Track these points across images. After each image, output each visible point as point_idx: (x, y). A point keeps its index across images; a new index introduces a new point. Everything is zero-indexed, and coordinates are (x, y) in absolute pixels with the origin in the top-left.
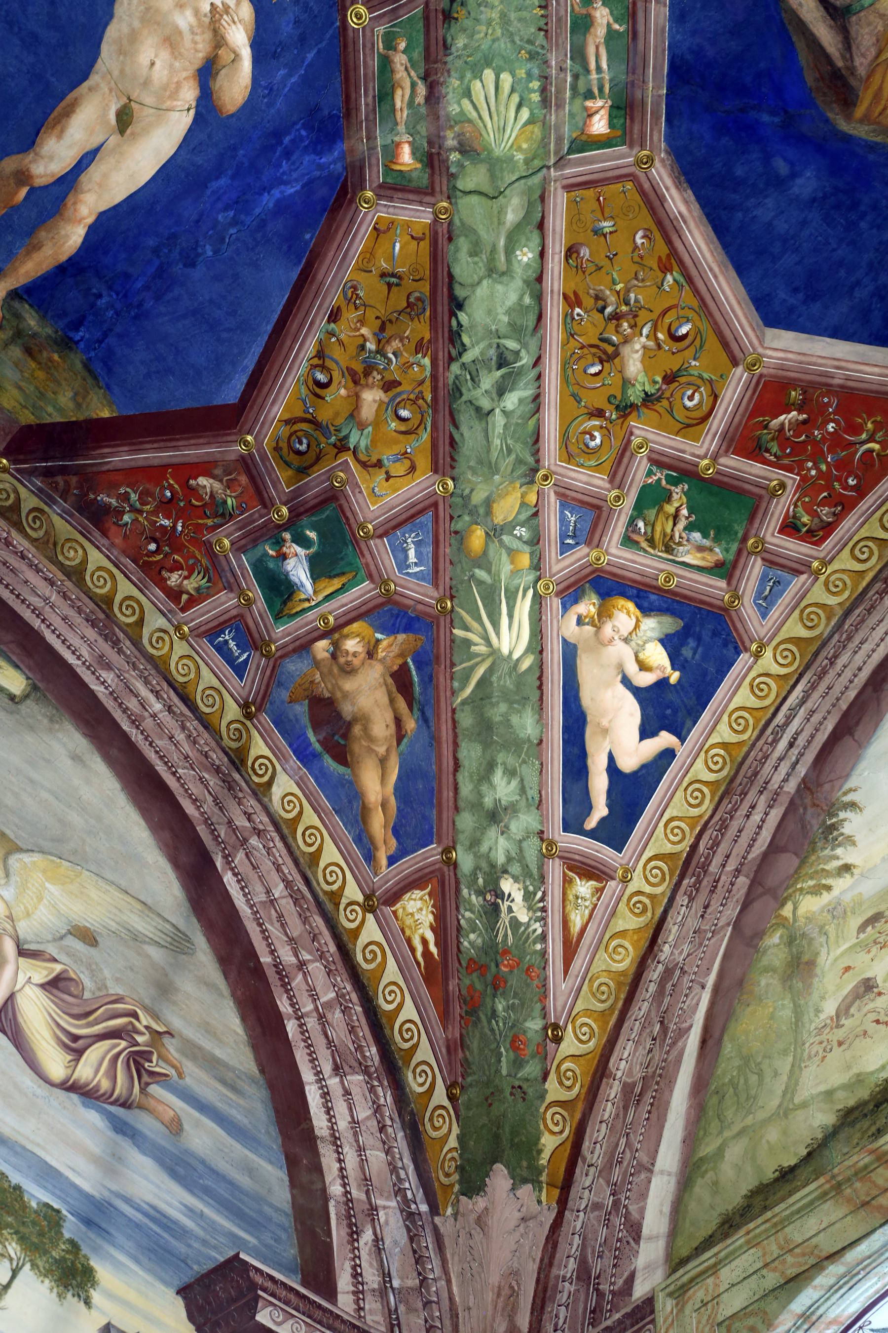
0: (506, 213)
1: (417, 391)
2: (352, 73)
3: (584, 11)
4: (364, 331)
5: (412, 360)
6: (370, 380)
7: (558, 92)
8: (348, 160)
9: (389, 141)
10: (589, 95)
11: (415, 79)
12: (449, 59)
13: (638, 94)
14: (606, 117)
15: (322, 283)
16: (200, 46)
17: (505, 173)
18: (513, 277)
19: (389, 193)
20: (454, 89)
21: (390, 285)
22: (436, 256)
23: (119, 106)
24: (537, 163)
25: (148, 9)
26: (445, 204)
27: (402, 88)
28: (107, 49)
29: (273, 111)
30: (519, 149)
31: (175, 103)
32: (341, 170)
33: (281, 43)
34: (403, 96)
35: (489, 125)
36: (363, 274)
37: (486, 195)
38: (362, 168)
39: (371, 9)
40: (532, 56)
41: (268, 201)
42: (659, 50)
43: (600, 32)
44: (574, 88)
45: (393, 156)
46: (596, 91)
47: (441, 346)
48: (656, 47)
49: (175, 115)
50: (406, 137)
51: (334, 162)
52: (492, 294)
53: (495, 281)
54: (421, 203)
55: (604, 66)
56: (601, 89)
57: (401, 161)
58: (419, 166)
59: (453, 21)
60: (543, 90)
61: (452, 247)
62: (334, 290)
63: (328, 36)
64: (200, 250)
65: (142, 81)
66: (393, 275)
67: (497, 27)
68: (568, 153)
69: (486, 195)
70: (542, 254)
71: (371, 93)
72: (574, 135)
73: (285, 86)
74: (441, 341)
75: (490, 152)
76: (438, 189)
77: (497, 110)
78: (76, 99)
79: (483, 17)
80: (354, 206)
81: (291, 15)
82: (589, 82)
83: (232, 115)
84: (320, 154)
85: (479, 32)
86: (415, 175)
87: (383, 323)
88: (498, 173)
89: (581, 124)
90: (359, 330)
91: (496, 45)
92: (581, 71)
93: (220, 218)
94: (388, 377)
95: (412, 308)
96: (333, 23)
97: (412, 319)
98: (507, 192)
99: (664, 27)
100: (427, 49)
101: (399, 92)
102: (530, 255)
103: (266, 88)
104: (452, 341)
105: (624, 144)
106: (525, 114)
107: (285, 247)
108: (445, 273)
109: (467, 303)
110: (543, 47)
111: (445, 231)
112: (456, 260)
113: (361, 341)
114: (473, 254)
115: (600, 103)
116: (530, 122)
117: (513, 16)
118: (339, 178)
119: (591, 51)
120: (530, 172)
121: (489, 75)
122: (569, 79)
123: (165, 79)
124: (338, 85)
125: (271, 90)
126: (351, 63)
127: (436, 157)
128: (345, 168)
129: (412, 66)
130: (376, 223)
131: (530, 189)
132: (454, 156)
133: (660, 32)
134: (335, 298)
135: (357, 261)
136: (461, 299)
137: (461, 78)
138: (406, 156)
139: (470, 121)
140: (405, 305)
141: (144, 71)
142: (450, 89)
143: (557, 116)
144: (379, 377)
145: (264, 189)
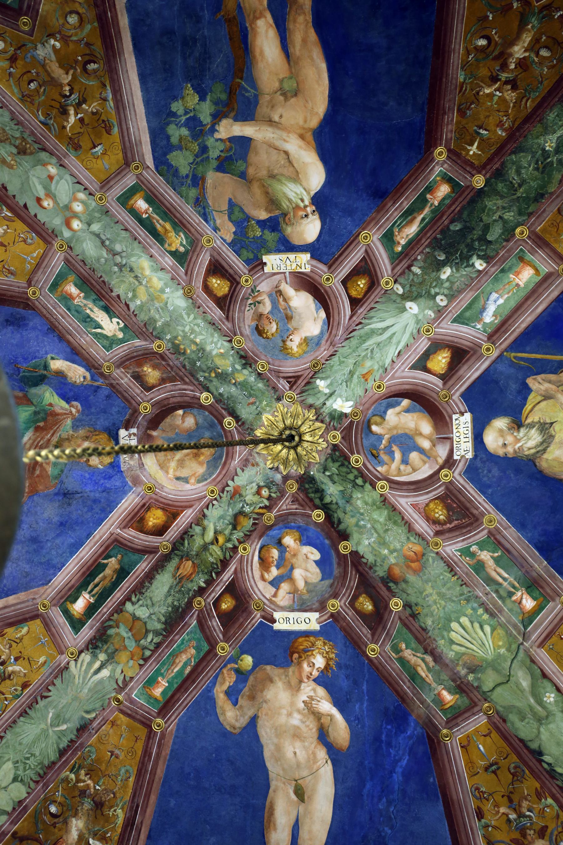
0: (521, 684)
1: (559, 824)
2: (390, 679)
3: (475, 561)
4: (502, 810)
5: (541, 807)
6: (529, 838)
7: (494, 605)
8: (421, 722)
9: (433, 696)
10: (511, 594)
11: (422, 656)
12: (430, 634)
13: (534, 574)
14: (528, 597)
15: (459, 800)
16: (311, 726)
17: (503, 664)
18: (554, 715)
19: (454, 722)
20: (444, 646)
21: (494, 772)
22: (505, 736)
23: (293, 788)
24: (514, 646)
25: (276, 729)
26: (487, 705)
27: (419, 666)
28: (269, 765)
29: (366, 729)
30: (499, 647)
31: (318, 764)
32: (421, 731)
33: (346, 692)
34: (422, 669)
35: (475, 648)
36: (475, 777)
37: (503, 683)
38: (430, 721)
39: (376, 643)
40: (468, 600)
41: (397, 777)
42: (525, 547)
43: (491, 563)
44: (500, 597)
45: (441, 702)
46: (513, 590)
47: (550, 785)
48: (522, 547)
49: (322, 771)
50: (440, 688)
51: (415, 729)
52: (551, 732)
53: (547, 724)
54: (474, 714)
55: (506, 575)
56: (514, 587)
57: (446, 702)
58: (457, 696)
59: (418, 616)
60: (487, 610)
61: (509, 724)
62: (468, 799)
63: (366, 671)
64: (383, 834)
65: (295, 766)
66: (492, 765)
67: (440, 601)
68: (525, 629)
69: (503, 683)
70: (558, 690)
71: (406, 681)
72: (521, 618)
73: (363, 711)
74: (547, 782)
75: (486, 660)
76: (476, 700)
77: (472, 638)
78: (271, 802)
79: (430, 602)
80: (442, 744)
81: (342, 676)
82: (505, 589)
83: (349, 747)
84: (404, 731)
85: (434, 611)
86: (459, 702)
87: (509, 797)
88: (500, 668)
89: (519, 610)
90: (498, 812)
91: (446, 609)
92: (497, 587)
93: (381, 807)
94: (537, 828)
95: (516, 776)
96: (364, 663)
97: (522, 782)
98: (512, 673)
99: (519, 537)
100: (416, 638)
101: (419, 669)
102: (553, 695)
103: (355, 720)
104: (553, 778)
105: (549, 602)
106: (487, 629)
107: (425, 796)
108: (517, 741)
109: (542, 749)
110: (470, 592)
111: (498, 719)
112: (517, 729)
113: (505, 818)
114: (523, 719)
115: (519, 594)
116: (493, 630)
117: (444, 590)
118: (423, 735)
119: (494, 574)
120: (515, 653)
121: (454, 625)
122: (494, 595)
123: (306, 756)
124: (388, 690)
125: (358, 719)
126: (386, 674)
127: (462, 685)
128: (423, 728)
129: (416, 651)
130: (460, 744)
131: (523, 662)
132: (471, 677)
133: (519, 540)
134: (472, 804)
135: (467, 773)
136: (537, 749)
137: (443, 638)
138: (447, 697)
139: (464, 654)
140: (511, 776)
141: (294, 760)
142: (442, 647)
143: (504, 617)
144: (532, 832)
145: (392, 772)
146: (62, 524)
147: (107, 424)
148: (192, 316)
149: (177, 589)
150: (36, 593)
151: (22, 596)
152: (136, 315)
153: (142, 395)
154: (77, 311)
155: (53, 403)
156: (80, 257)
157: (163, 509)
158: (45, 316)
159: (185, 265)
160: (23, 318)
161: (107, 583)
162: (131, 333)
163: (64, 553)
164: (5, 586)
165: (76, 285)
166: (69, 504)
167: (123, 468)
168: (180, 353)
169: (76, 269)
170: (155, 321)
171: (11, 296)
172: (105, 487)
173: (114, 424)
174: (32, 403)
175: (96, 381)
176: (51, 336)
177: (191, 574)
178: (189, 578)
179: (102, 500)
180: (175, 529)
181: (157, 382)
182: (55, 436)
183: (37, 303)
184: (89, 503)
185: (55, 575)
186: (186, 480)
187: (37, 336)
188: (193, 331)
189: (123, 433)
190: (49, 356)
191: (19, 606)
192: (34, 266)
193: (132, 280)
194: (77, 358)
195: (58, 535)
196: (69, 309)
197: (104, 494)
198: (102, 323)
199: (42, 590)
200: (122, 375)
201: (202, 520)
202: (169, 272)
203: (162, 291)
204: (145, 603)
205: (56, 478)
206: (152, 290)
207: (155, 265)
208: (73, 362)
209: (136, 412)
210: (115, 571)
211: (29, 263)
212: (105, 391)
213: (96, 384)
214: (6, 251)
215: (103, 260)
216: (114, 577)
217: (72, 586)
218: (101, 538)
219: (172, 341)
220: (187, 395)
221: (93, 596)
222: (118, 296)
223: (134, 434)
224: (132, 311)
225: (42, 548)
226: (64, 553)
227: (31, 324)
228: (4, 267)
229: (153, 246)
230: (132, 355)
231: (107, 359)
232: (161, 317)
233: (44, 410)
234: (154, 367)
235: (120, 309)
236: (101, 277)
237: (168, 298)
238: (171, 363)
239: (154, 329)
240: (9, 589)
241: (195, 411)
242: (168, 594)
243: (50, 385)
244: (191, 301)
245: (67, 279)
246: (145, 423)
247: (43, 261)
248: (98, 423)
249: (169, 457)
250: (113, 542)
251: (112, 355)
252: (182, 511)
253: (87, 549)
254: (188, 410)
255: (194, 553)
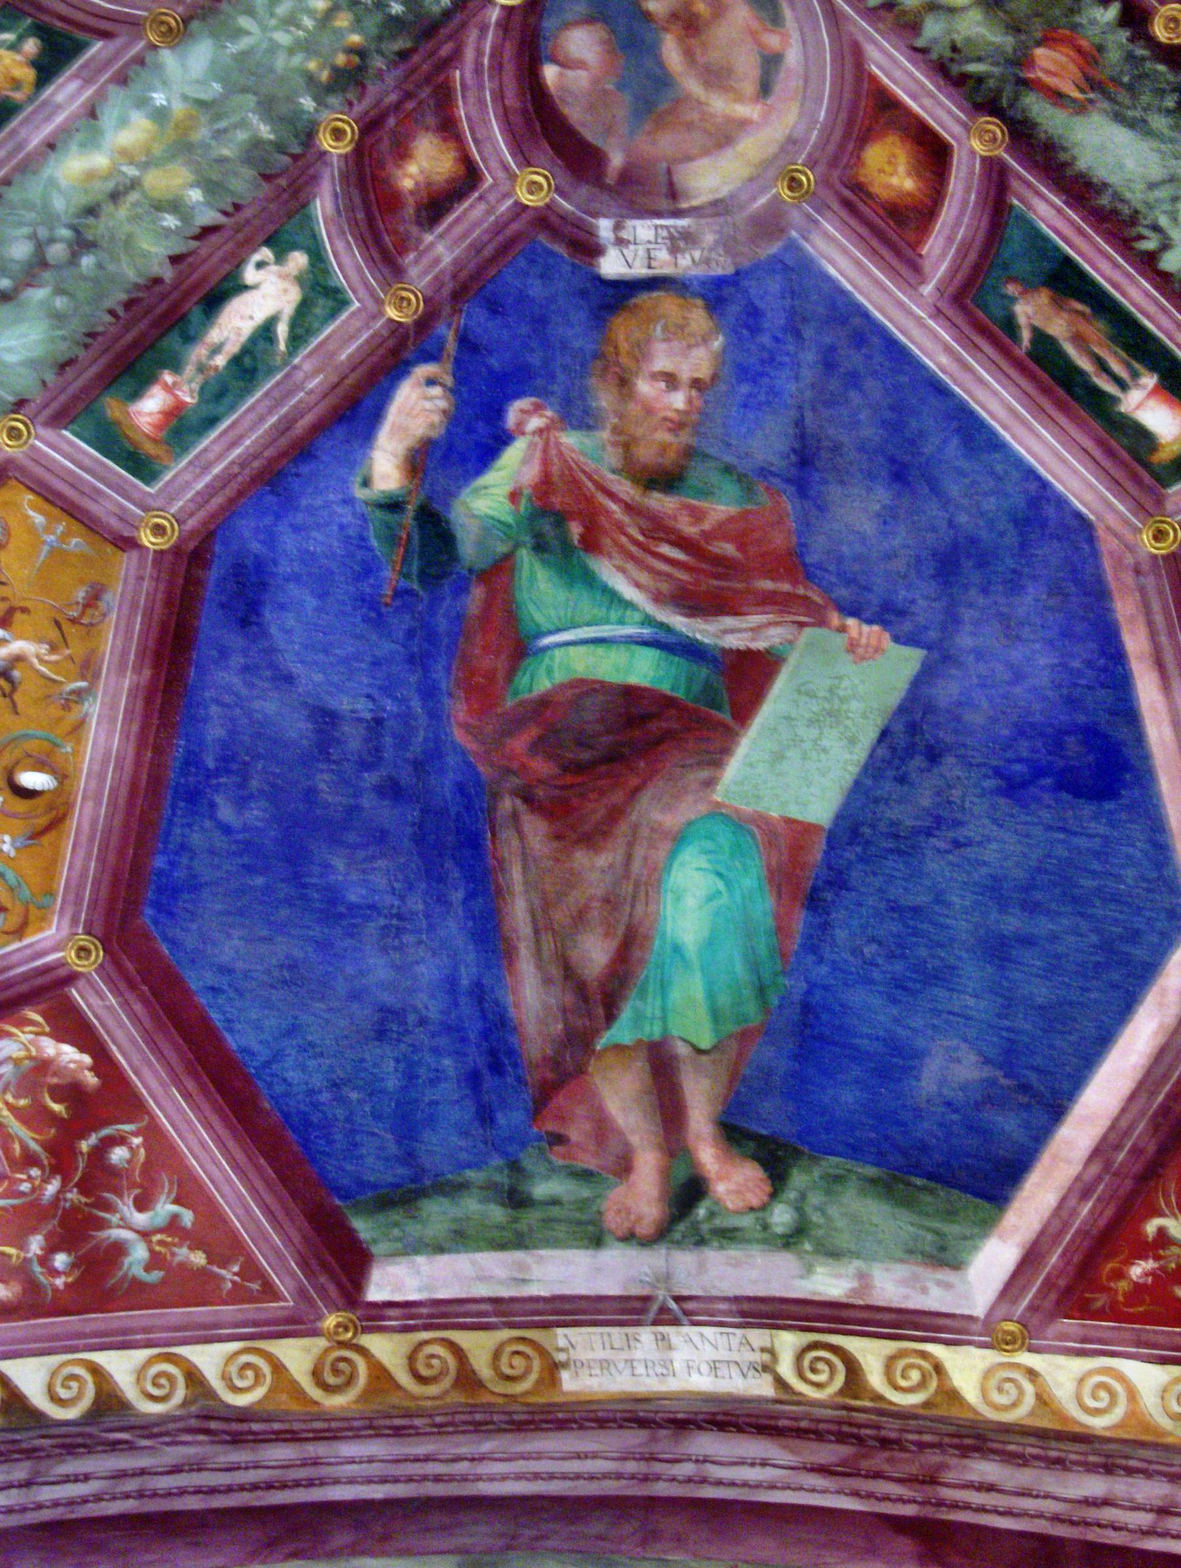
146: (900, 475)
147: (579, 316)
148: (244, 22)
149: (1123, 97)
150: (1119, 561)
151: (1125, 609)
152: (237, 207)
153: (492, 197)
154: (220, 395)
155: (507, 489)
156: (50, 377)
157: (864, 139)
158: (232, 501)
159: (80, 36)
160: (238, 570)
161: (1096, 330)
162: (292, 226)
163: (992, 473)
164: (1089, 664)
165: (136, 394)
166: (836, 448)
167: (723, 267)
168: (361, 69)
169: (85, 389)
170: (257, 143)
171: (168, 603)
172: (785, 329)
173: (584, 294)
174: (508, 557)
175: (441, 349)
176: (295, 485)
177: (1079, 50)
178: (1089, 58)
179: (828, 340)
180: (927, 102)
181: (452, 145)
182: (615, 488)
183: (191, 523)
184: (834, 384)
185: (1061, 502)
186: (771, 62)
187: (296, 529)
188: (291, 21)
189: (611, 265)
190: (360, 493)
191: (1159, 619)
192: (76, 527)
193: (123, 212)
194: (369, 403)
195: (935, 488)
196: (212, 422)
197: (808, 332)
198: (260, 316)
199: (1107, 544)
200: (425, 261)
201: (904, 13)
202: (101, 94)
203: (160, 115)
204: (1167, 207)
205: (749, 491)
206: (157, 150)
207: (79, 137)
208: (376, 416)
209: (544, 220)
210: (1058, 304)
211: (64, 537)
212: (476, 317)
213: (451, 346)
214: (24, 610)
215: (60, 303)
216: (1079, 306)
217: (1100, 442)
218: (948, 349)
219: (321, 92)
220: (496, 53)
221: (1135, 375)
222: (175, 260)
223: (618, 227)
224: (223, 220)
225: (973, 541)
226: (992, 473)
227: (255, 547)
228: (74, 621)
229: (19, 138)
230: (364, 227)
231: (371, 305)
232: (243, 124)
233: (532, 518)
234: (402, 153)
235: (215, 260)
236: (112, 312)
237: (185, 98)
238: (393, 98)
239: (280, 148)
240: (1103, 653)
241: (549, 24)
242: (1138, 126)
243: (450, 495)
244: (195, 25)
245: (117, 423)
246: (584, 191)
247: (59, 495)
248: (577, 344)
249: (695, 116)
250: (963, 308)
251: (362, 293)
252: (873, 79)
253: (981, 394)
254: (546, 47)
255: (1007, 42)
